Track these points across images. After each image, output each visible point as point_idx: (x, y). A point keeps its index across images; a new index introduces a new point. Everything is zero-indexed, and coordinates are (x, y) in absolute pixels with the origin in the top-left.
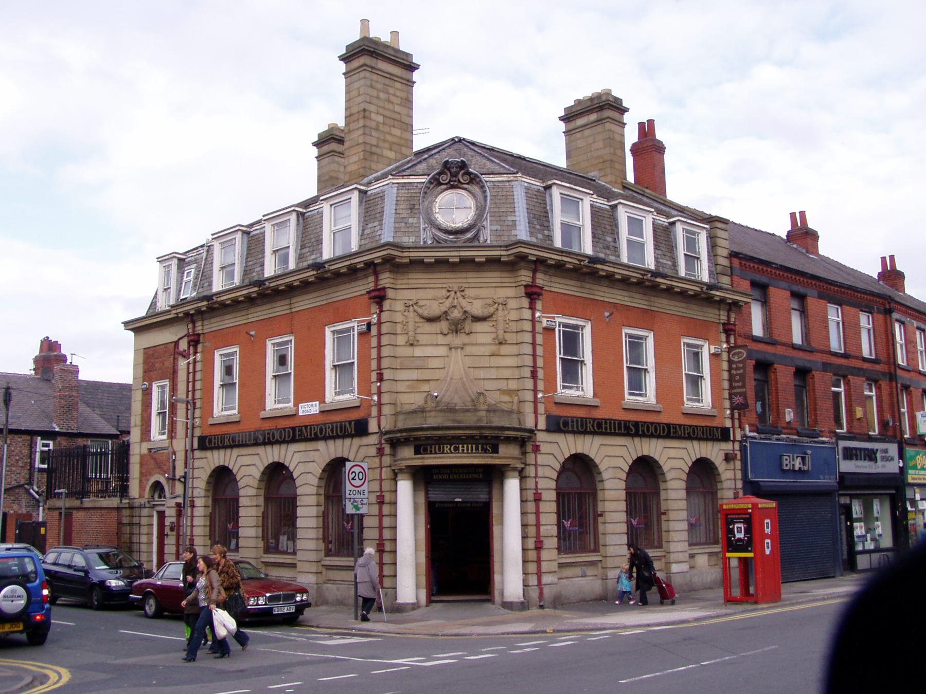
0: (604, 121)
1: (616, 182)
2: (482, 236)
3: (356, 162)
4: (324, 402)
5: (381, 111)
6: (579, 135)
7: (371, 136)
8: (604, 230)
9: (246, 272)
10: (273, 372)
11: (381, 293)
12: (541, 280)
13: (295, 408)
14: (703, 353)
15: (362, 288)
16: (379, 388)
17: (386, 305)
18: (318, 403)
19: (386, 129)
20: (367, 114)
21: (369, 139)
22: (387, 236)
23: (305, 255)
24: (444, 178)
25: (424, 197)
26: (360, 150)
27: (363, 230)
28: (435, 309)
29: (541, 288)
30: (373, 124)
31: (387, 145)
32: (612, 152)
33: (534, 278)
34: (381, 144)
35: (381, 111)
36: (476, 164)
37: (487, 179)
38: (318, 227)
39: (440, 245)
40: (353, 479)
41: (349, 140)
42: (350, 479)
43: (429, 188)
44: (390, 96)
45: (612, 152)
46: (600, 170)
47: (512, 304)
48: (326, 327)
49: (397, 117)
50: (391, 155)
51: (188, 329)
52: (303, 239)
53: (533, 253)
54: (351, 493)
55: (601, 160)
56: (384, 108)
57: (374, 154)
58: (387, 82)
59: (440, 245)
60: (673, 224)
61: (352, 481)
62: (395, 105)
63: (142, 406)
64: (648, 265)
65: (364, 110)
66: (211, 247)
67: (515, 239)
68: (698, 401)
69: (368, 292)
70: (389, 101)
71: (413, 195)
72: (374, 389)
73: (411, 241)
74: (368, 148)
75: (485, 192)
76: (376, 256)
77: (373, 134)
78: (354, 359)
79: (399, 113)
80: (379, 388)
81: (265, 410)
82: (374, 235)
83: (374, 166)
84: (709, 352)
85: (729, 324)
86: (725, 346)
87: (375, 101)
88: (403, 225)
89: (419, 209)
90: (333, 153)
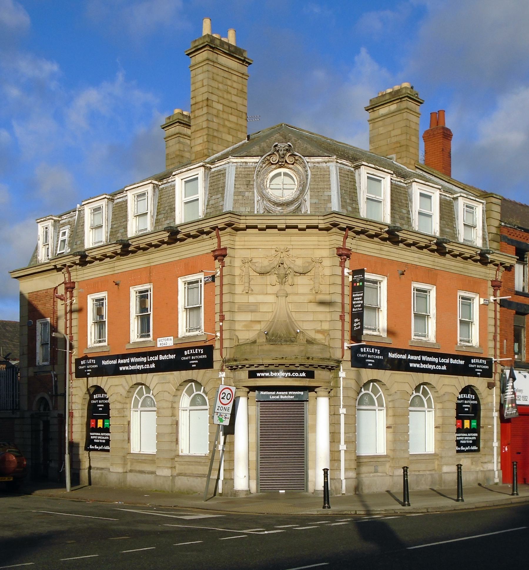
0: (402, 111)
1: (410, 164)
2: (303, 207)
3: (201, 144)
4: (177, 337)
5: (221, 100)
6: (381, 123)
7: (213, 122)
8: (400, 204)
9: (113, 233)
10: (136, 314)
11: (223, 253)
12: (351, 244)
13: (154, 341)
14: (474, 304)
15: (208, 247)
16: (221, 327)
17: (226, 260)
18: (172, 338)
19: (225, 116)
20: (210, 102)
21: (211, 125)
22: (228, 206)
23: (161, 220)
24: (274, 160)
25: (257, 175)
26: (204, 134)
27: (208, 201)
28: (264, 263)
29: (350, 250)
30: (215, 112)
31: (226, 130)
32: (408, 138)
33: (344, 242)
34: (221, 129)
35: (221, 100)
36: (299, 147)
37: (308, 160)
38: (171, 197)
39: (270, 214)
40: (223, 398)
41: (195, 125)
42: (221, 398)
43: (262, 167)
44: (229, 87)
45: (408, 138)
46: (397, 153)
47: (327, 262)
48: (179, 278)
49: (233, 105)
50: (230, 138)
51: (65, 278)
52: (159, 207)
53: (344, 222)
54: (219, 409)
55: (399, 145)
56: (223, 98)
57: (215, 137)
58: (226, 75)
59: (270, 214)
60: (456, 199)
61: (222, 400)
62: (233, 96)
63: (28, 339)
64: (434, 232)
65: (207, 99)
66: (82, 212)
67: (330, 211)
68: (469, 342)
69: (213, 251)
70: (228, 92)
71: (249, 173)
72: (218, 328)
73: (247, 210)
74: (211, 132)
75: (306, 171)
76: (220, 222)
77: (215, 121)
78: (201, 304)
79: (235, 102)
80: (221, 327)
81: (129, 343)
82: (217, 205)
83: (215, 147)
84: (479, 303)
85: (496, 280)
86: (492, 299)
87: (215, 91)
88: (240, 197)
89: (253, 185)
90: (179, 135)
